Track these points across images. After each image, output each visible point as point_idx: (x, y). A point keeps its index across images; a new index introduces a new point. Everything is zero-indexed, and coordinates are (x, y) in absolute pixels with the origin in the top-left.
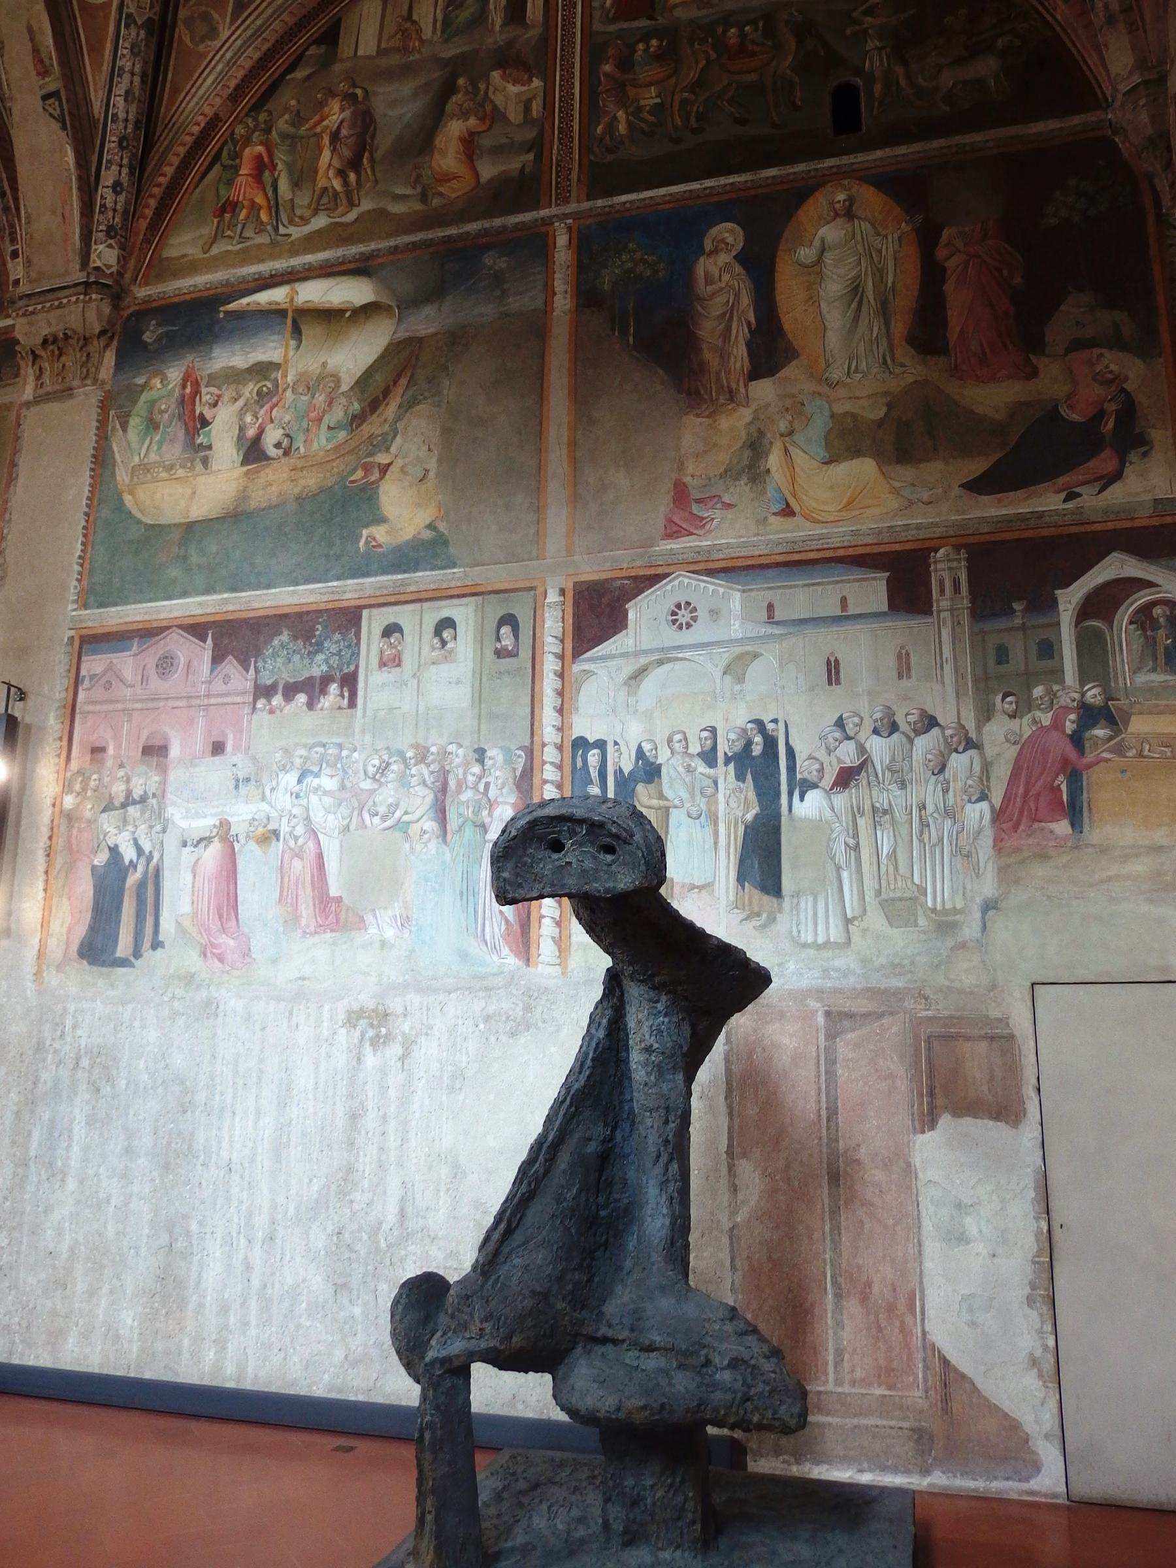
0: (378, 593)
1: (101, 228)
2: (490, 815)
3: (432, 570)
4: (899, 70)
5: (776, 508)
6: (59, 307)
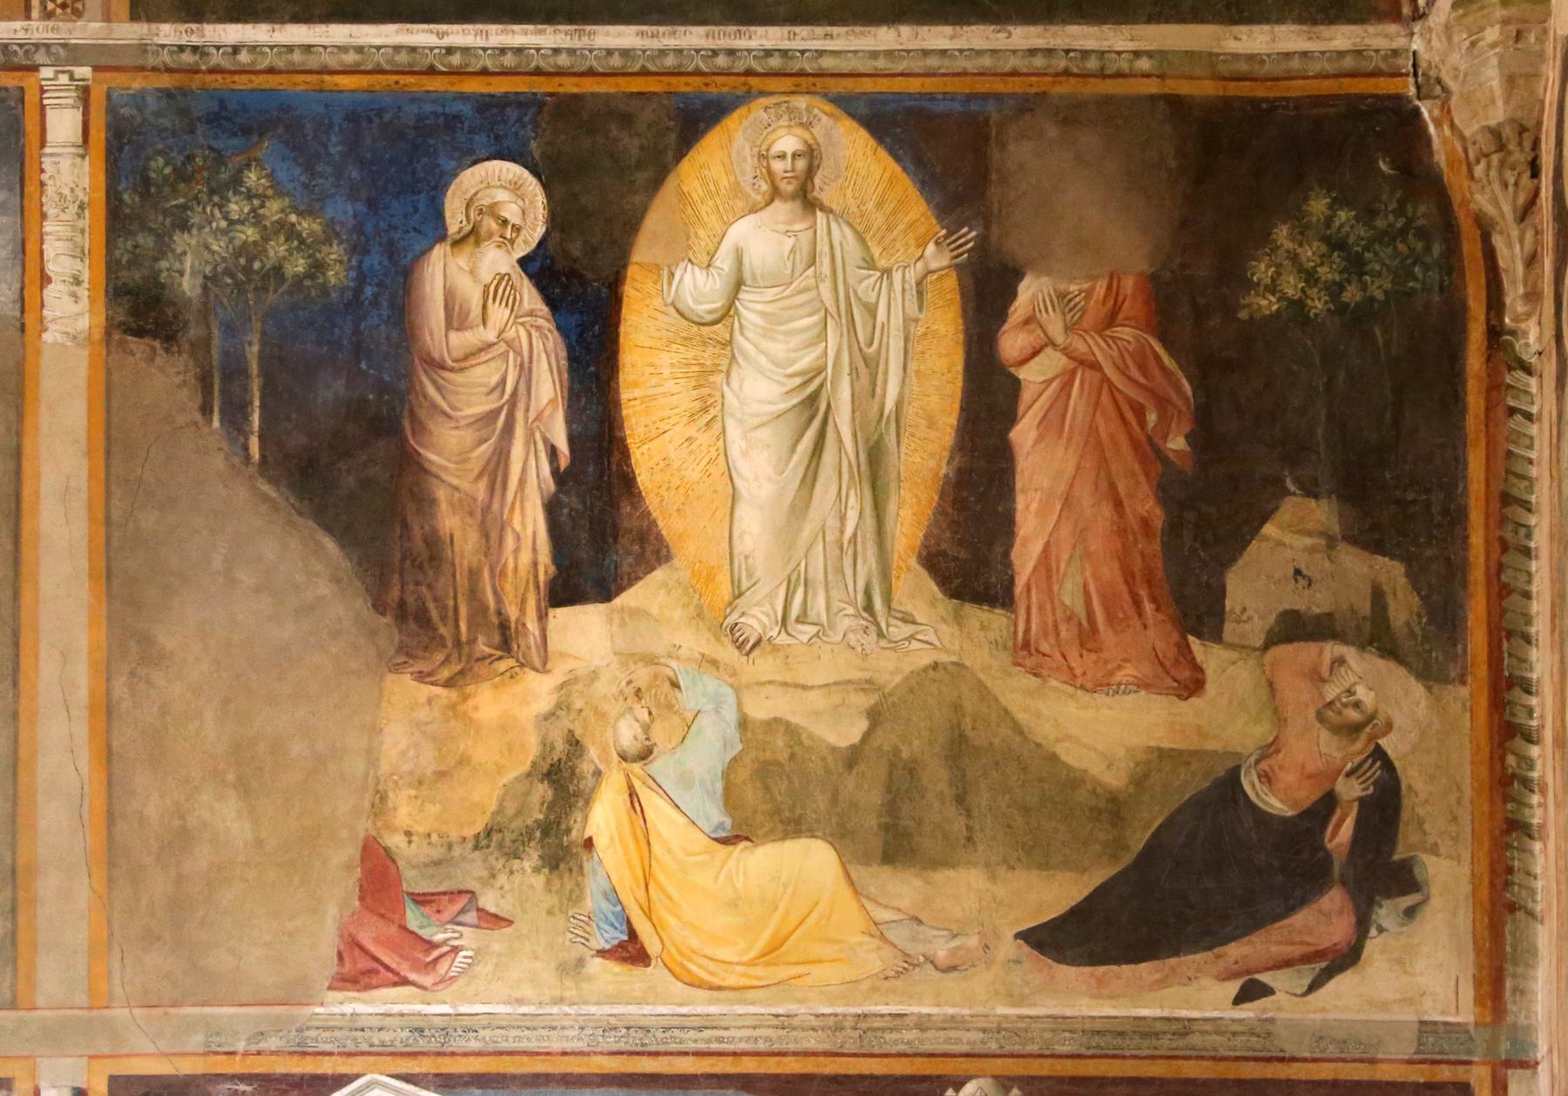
5: (611, 936)
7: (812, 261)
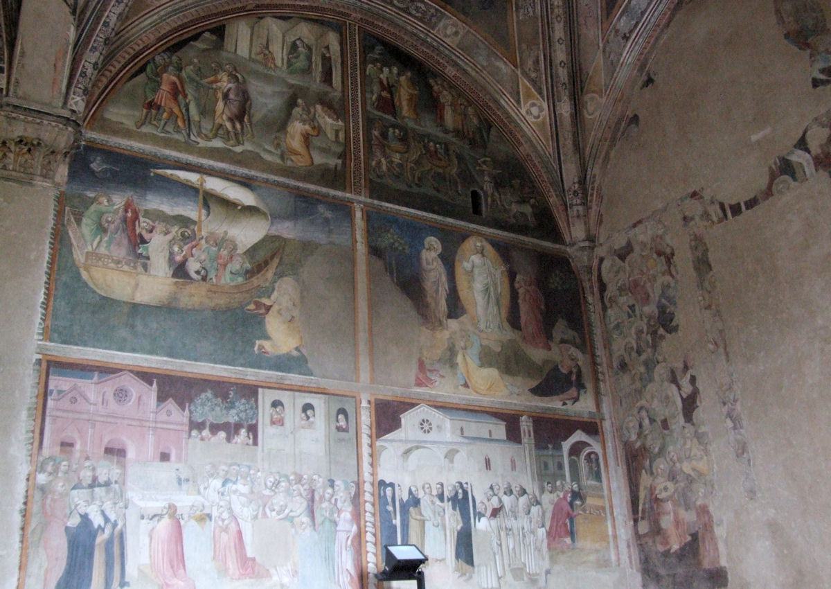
0: (268, 380)
1: (80, 86)
2: (339, 516)
3: (300, 374)
4: (496, 194)
5: (462, 382)
6: (38, 124)
7: (485, 264)
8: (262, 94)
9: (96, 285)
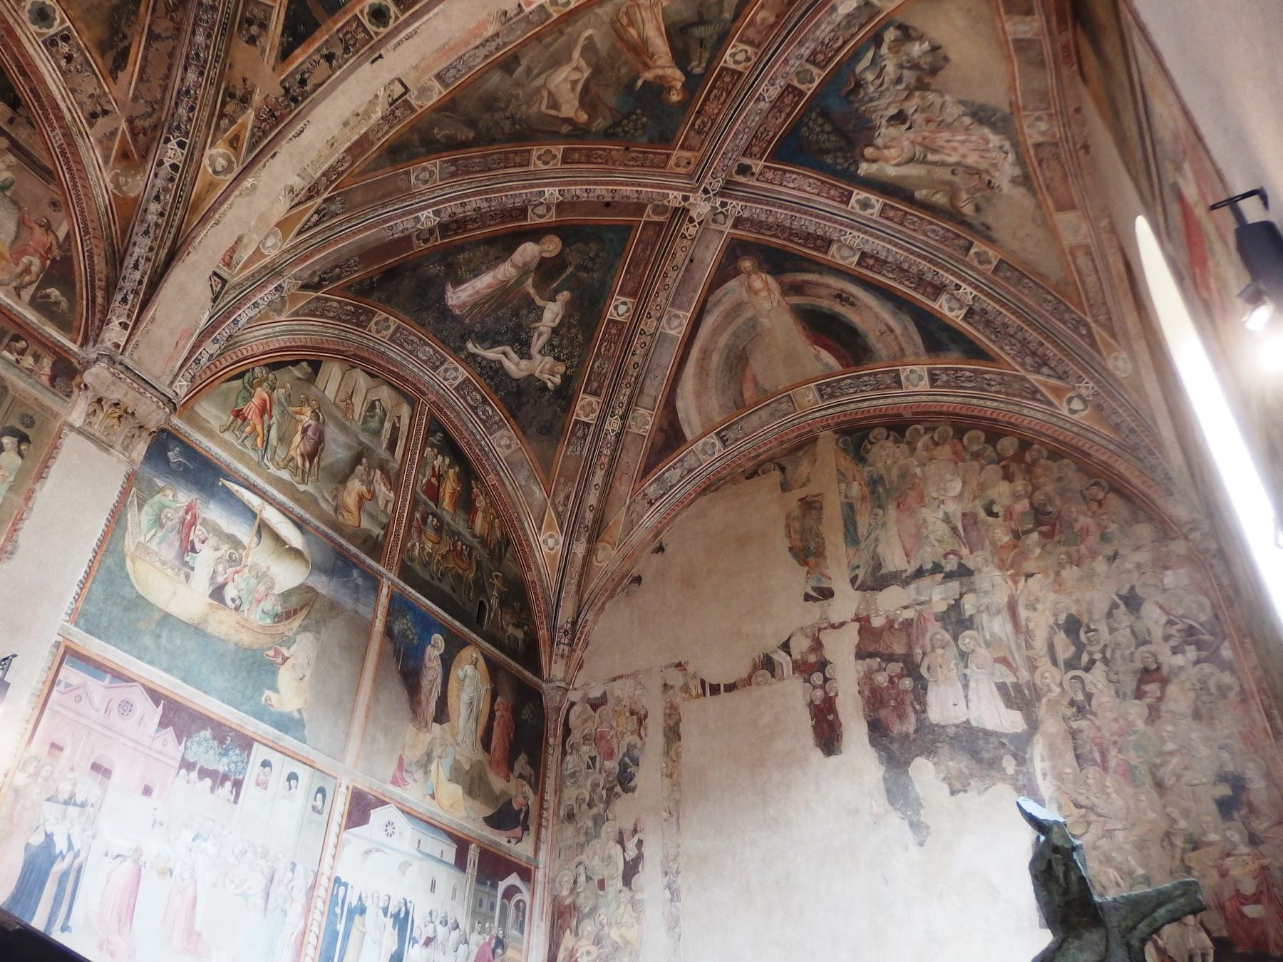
6: (141, 393)
8: (335, 441)
9: (137, 580)
